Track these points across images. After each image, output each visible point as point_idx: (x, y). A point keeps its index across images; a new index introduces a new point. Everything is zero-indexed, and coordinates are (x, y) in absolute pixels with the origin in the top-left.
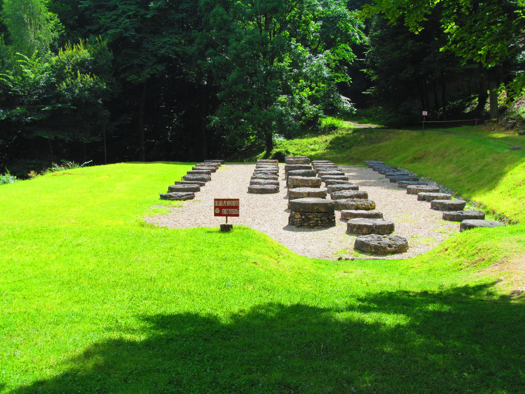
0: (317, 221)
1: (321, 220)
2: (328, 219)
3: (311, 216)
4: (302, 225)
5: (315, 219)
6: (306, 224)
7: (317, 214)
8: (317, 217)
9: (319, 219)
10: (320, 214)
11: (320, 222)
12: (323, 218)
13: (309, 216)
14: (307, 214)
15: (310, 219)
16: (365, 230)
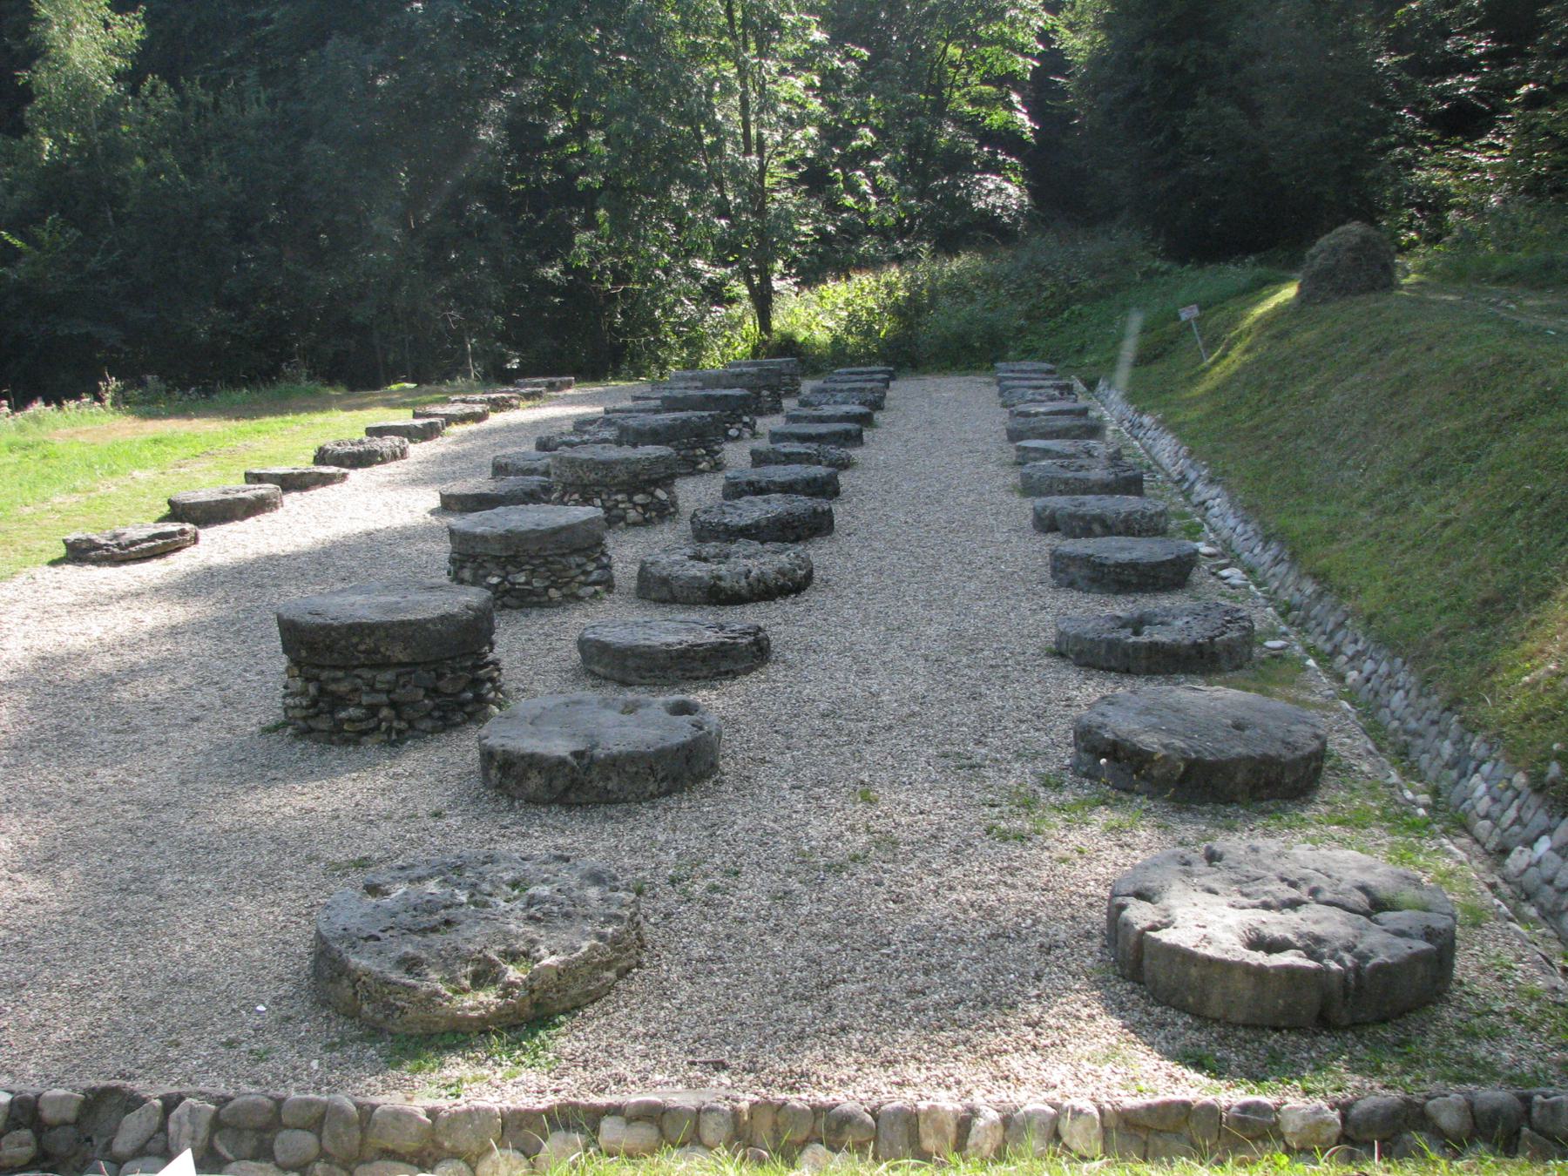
0: (373, 710)
1: (393, 705)
2: (433, 692)
3: (343, 687)
4: (310, 730)
5: (365, 700)
6: (324, 724)
7: (367, 674)
8: (373, 689)
9: (384, 698)
10: (389, 675)
11: (385, 712)
12: (399, 694)
13: (333, 687)
14: (325, 675)
15: (339, 701)
16: (535, 781)
